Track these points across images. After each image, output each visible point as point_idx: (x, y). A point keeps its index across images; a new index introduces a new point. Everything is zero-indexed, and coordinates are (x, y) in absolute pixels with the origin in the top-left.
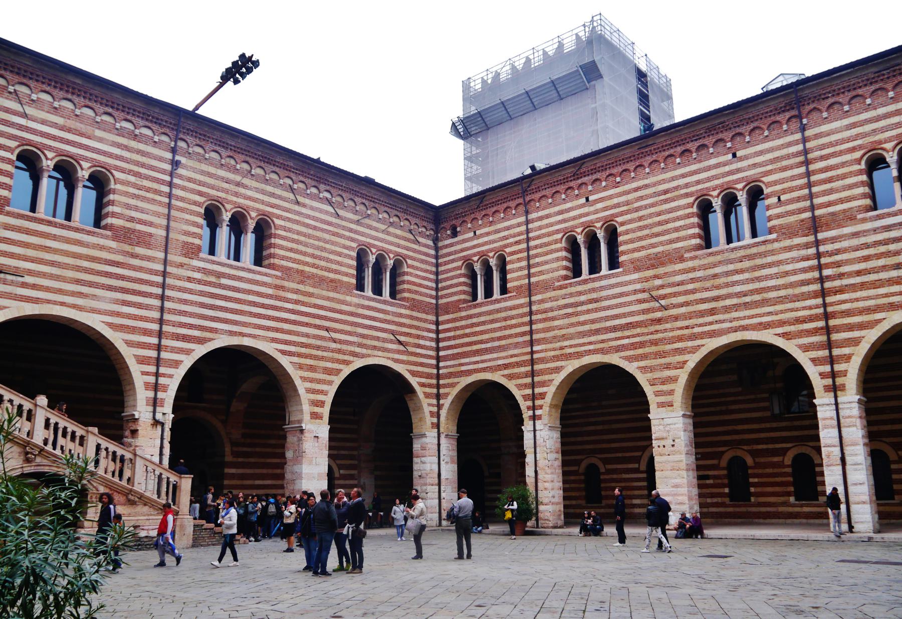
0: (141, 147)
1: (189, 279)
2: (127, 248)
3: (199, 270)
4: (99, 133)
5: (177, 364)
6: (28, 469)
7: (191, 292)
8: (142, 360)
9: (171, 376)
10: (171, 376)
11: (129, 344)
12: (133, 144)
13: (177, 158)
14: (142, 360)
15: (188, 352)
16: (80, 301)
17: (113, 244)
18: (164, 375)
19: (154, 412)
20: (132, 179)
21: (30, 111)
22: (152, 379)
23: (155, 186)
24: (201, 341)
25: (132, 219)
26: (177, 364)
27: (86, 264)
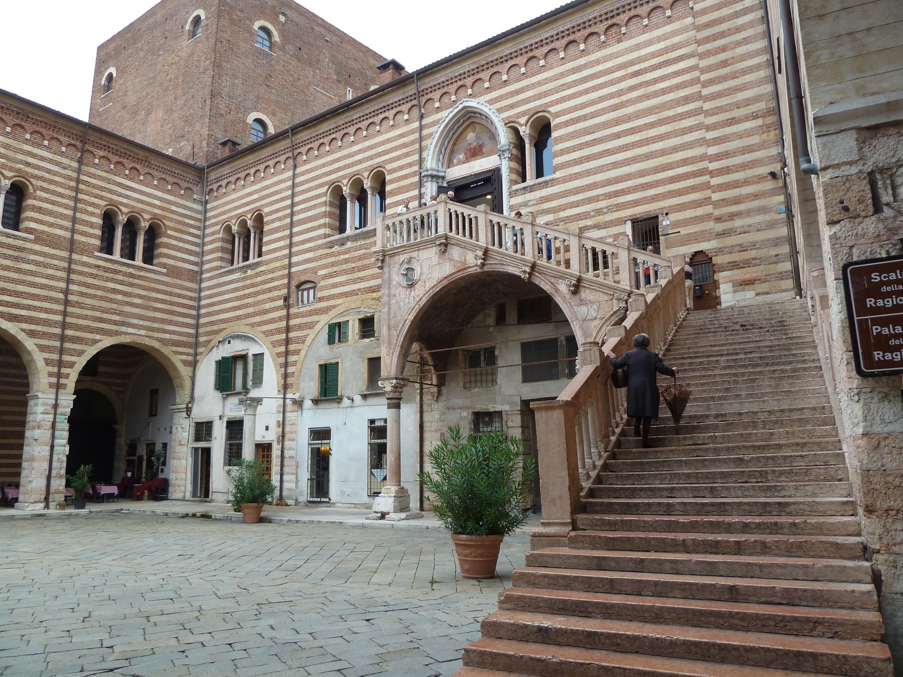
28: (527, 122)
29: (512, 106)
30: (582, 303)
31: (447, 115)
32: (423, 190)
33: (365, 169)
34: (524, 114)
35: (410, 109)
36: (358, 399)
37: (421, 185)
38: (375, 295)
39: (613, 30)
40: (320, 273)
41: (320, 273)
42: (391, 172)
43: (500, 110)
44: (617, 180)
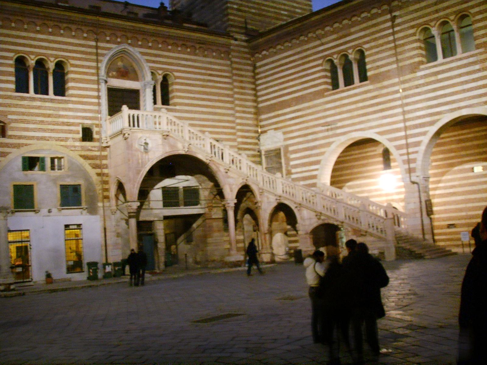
0: (374, 22)
1: (417, 87)
2: (379, 85)
3: (422, 77)
4: (353, 30)
5: (418, 144)
6: (320, 222)
7: (419, 94)
8: (398, 148)
9: (416, 152)
10: (416, 152)
11: (391, 140)
12: (370, 23)
13: (394, 14)
14: (398, 148)
15: (424, 134)
16: (362, 126)
17: (371, 87)
18: (413, 153)
19: (410, 177)
20: (373, 44)
21: (324, 40)
22: (405, 157)
23: (386, 40)
24: (432, 123)
25: (378, 67)
26: (418, 144)
27: (361, 105)
28: (162, 74)
29: (154, 62)
30: (229, 177)
31: (115, 48)
32: (100, 86)
33: (52, 55)
34: (161, 69)
35: (88, 31)
36: (55, 211)
37: (98, 83)
38: (63, 143)
39: (201, 50)
40: (10, 117)
41: (10, 117)
42: (73, 65)
43: (148, 61)
44: (204, 120)
